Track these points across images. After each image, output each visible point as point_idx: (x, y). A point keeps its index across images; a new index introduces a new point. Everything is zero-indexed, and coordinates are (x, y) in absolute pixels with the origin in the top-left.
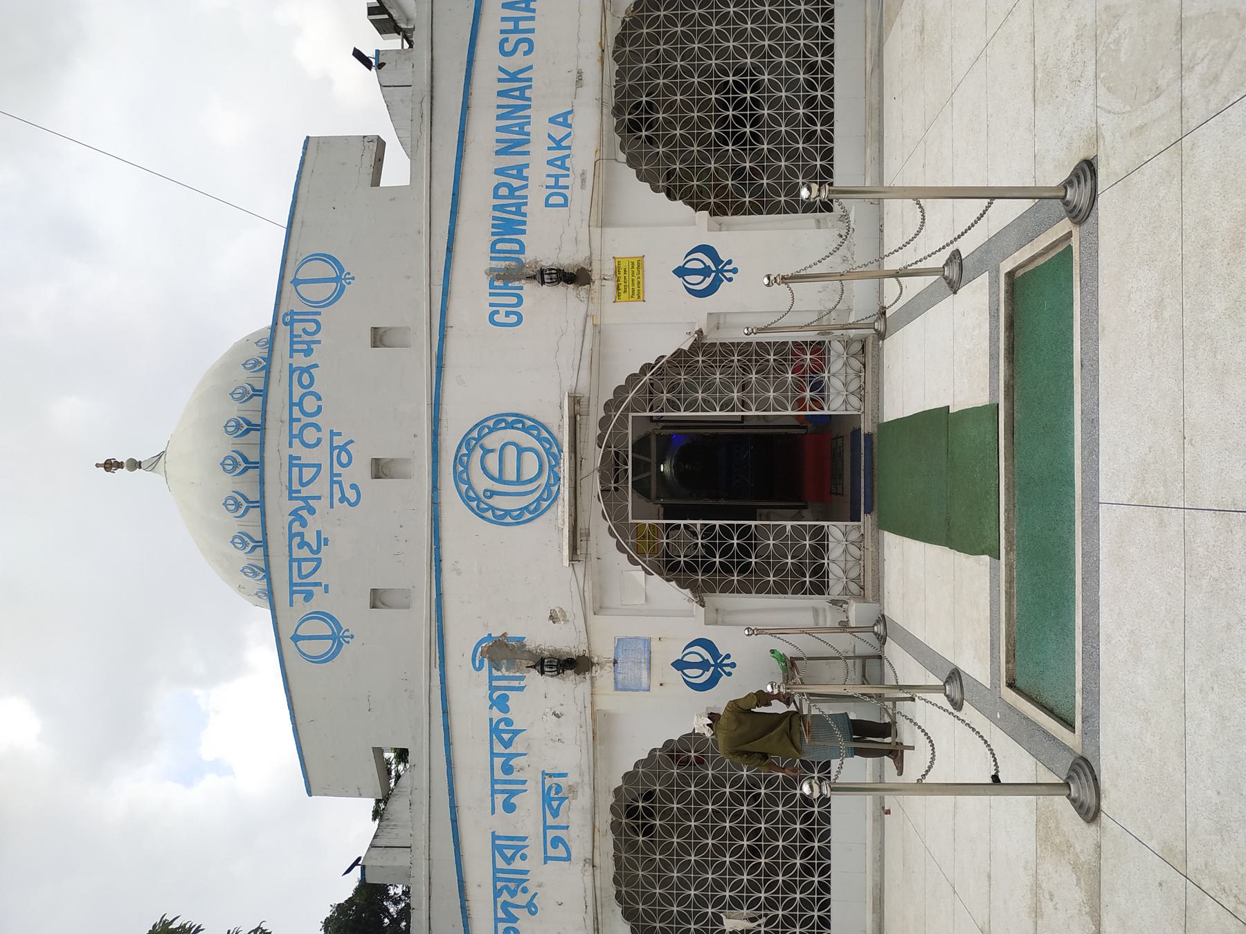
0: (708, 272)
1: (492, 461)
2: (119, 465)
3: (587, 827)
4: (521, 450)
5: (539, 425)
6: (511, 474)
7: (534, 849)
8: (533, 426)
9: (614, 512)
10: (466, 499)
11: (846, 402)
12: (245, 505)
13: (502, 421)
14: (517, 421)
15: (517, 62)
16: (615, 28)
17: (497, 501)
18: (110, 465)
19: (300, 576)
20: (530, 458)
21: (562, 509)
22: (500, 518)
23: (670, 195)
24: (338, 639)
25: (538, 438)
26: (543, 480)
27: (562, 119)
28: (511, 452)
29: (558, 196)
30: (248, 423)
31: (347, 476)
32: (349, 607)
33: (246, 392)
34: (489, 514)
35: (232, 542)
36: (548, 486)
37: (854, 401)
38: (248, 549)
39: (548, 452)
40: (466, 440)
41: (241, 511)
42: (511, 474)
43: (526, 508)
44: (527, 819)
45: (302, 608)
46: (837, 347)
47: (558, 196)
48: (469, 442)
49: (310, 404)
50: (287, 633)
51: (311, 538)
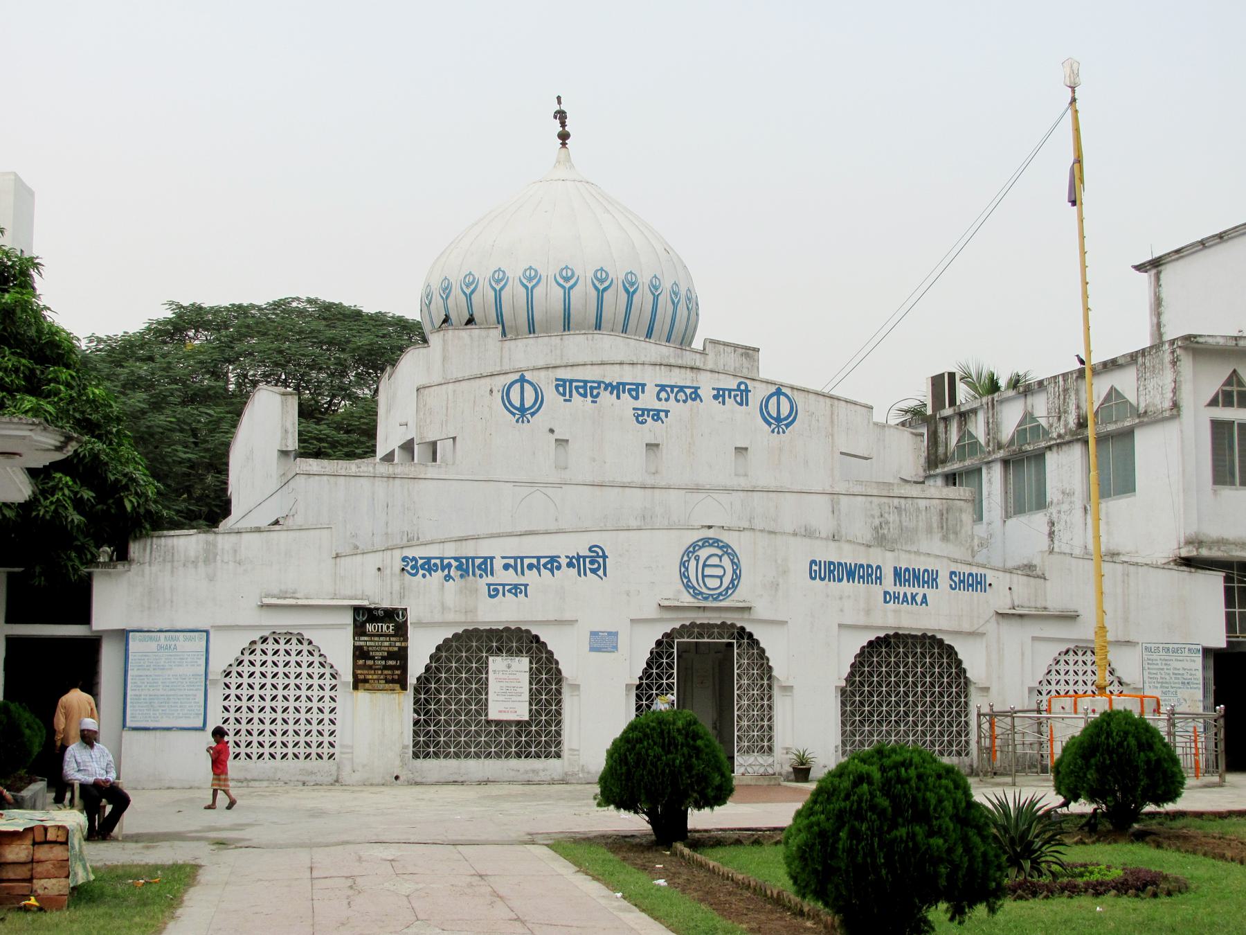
1: (715, 561)
2: (563, 125)
4: (721, 578)
5: (735, 587)
6: (708, 571)
8: (734, 585)
9: (684, 630)
10: (694, 545)
11: (741, 765)
12: (567, 285)
13: (736, 565)
14: (737, 576)
16: (939, 636)
17: (693, 563)
18: (561, 116)
19: (577, 388)
20: (716, 583)
21: (687, 599)
22: (683, 564)
23: (852, 665)
25: (728, 588)
26: (704, 590)
28: (720, 572)
30: (635, 292)
33: (656, 288)
34: (686, 558)
35: (531, 268)
36: (701, 593)
37: (742, 770)
38: (525, 282)
39: (720, 594)
40: (728, 546)
41: (562, 282)
42: (708, 571)
43: (689, 580)
46: (770, 760)
48: (726, 549)
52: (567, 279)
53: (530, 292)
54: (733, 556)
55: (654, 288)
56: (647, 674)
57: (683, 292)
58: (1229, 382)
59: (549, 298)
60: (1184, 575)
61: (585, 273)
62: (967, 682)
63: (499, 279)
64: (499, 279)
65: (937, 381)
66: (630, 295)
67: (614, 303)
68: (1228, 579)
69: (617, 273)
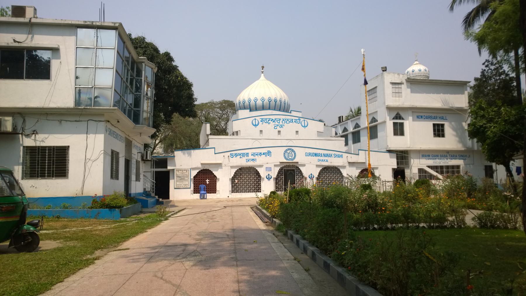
0: (311, 178)
3: (250, 164)
7: (247, 158)
8: (294, 158)
13: (295, 154)
15: (333, 156)
24: (256, 125)
27: (327, 161)
29: (319, 160)
31: (278, 127)
32: (259, 128)
44: (251, 157)
45: (260, 120)
47: (319, 160)
49: (288, 122)
50: (256, 118)
51: (269, 122)
52: (263, 100)
53: (256, 102)
54: (294, 152)
55: (280, 101)
56: (278, 175)
57: (286, 102)
58: (397, 114)
59: (259, 103)
60: (388, 155)
61: (266, 98)
62: (343, 176)
63: (250, 100)
64: (250, 100)
65: (340, 118)
66: (276, 102)
67: (273, 103)
68: (397, 154)
69: (273, 98)
